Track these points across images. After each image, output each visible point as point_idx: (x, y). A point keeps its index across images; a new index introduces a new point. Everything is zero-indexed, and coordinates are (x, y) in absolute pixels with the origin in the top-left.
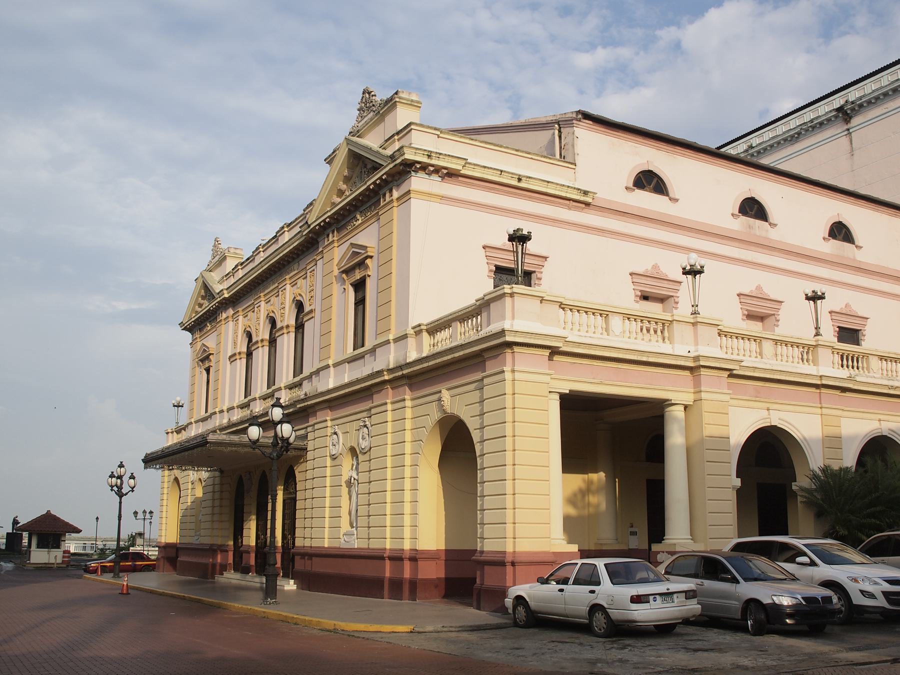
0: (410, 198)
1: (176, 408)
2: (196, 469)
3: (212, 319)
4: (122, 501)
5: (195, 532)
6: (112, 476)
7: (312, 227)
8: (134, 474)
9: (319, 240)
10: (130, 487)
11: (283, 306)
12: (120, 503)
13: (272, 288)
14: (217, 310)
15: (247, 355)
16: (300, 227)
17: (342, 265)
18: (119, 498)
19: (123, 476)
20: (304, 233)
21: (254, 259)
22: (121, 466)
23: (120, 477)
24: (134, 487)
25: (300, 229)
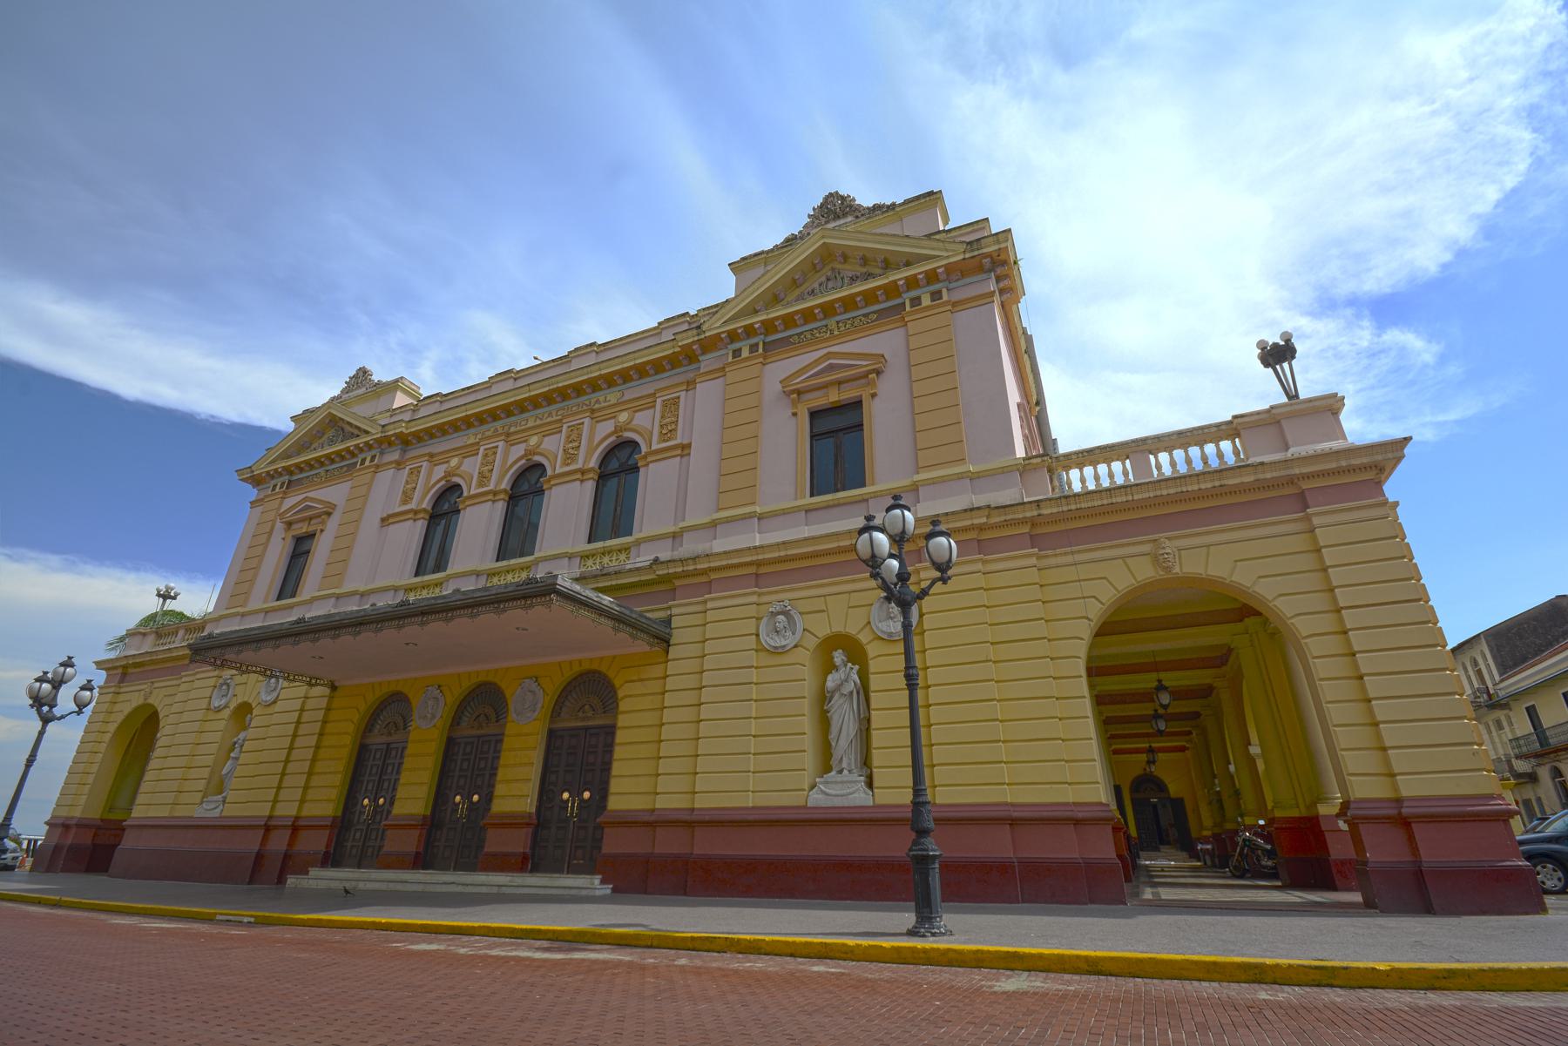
1: (161, 600)
3: (333, 466)
7: (707, 334)
8: (93, 683)
11: (576, 444)
12: (41, 733)
13: (531, 424)
14: (361, 450)
15: (431, 517)
16: (674, 334)
18: (41, 723)
19: (65, 683)
20: (680, 344)
21: (491, 386)
22: (68, 663)
23: (57, 684)
25: (673, 337)
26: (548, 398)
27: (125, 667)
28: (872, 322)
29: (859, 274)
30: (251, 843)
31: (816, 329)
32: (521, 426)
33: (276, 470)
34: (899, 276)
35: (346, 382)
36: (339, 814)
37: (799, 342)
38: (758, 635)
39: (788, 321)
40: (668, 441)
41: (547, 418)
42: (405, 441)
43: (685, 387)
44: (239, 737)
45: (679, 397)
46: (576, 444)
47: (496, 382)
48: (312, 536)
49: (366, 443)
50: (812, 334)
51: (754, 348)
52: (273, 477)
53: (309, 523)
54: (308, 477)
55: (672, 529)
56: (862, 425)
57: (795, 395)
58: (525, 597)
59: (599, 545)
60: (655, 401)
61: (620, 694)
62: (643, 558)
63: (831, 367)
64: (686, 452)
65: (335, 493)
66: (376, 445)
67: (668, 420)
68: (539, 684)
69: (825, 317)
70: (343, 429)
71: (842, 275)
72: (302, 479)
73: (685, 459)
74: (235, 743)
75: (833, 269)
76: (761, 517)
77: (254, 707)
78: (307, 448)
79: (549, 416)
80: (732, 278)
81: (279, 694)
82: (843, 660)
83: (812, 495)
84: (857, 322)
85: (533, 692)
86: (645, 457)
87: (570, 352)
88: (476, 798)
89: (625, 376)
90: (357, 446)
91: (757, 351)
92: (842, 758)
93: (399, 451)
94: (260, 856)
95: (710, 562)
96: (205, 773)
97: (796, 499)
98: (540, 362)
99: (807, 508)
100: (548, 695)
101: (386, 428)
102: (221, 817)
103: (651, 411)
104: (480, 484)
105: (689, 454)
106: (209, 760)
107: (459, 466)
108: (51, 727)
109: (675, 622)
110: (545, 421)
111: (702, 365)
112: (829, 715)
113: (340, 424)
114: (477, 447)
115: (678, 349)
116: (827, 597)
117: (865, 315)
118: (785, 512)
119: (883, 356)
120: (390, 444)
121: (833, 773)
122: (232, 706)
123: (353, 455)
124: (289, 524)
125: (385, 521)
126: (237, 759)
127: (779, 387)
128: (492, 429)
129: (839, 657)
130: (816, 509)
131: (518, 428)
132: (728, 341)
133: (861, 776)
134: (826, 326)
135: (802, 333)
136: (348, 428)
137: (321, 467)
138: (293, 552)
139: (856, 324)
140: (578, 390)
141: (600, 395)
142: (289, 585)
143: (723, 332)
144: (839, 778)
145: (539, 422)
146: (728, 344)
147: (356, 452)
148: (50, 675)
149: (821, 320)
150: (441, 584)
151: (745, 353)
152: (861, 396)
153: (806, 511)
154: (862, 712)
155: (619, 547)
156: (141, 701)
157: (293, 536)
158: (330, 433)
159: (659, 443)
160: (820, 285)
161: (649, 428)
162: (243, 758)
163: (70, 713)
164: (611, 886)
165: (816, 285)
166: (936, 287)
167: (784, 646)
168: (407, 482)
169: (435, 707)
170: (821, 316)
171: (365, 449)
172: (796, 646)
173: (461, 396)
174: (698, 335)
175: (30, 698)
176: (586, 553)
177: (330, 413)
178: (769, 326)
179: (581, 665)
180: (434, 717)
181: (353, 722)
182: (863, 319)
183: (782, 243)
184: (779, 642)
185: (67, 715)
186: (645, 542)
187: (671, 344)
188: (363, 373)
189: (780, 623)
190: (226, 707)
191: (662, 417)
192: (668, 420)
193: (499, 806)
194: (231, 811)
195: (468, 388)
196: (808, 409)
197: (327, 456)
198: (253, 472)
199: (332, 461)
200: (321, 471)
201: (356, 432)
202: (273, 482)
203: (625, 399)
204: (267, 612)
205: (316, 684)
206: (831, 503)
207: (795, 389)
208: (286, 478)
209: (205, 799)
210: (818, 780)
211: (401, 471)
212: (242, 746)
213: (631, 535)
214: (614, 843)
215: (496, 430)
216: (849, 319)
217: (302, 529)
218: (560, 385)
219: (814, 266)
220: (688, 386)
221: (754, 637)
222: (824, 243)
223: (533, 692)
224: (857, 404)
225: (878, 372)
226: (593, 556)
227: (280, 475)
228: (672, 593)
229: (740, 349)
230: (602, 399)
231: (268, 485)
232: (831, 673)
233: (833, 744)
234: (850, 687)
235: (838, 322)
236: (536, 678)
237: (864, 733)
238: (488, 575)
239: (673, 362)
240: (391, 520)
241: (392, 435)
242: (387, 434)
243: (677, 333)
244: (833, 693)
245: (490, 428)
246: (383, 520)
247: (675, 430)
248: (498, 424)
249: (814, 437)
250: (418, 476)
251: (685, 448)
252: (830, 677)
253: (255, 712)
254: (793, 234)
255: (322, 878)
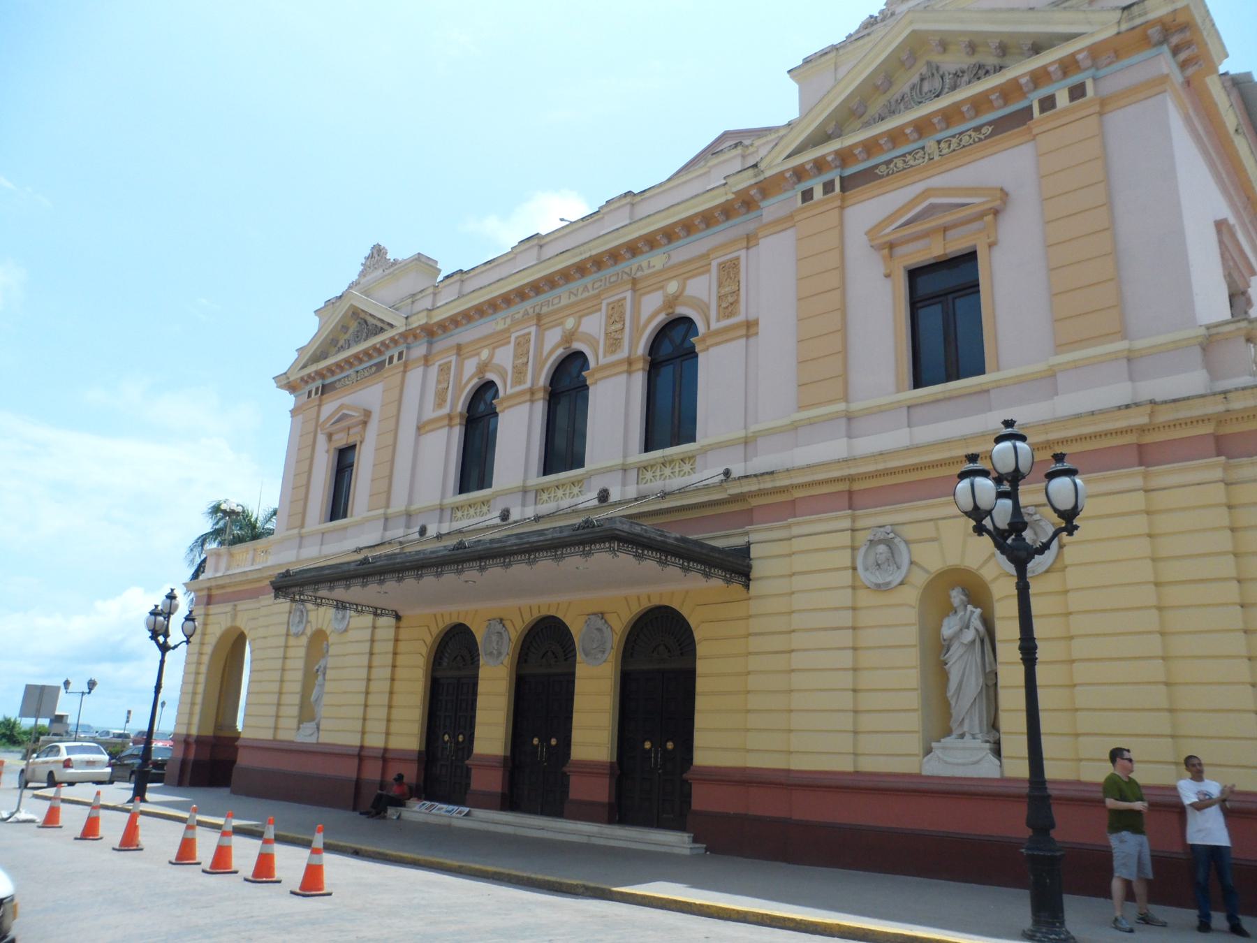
0: (1165, 91)
2: (359, 608)
3: (364, 366)
4: (167, 658)
5: (300, 722)
6: (154, 613)
7: (768, 174)
9: (762, 204)
10: (185, 635)
11: (618, 326)
12: (162, 662)
13: (564, 302)
14: (387, 347)
16: (725, 178)
17: (883, 233)
20: (734, 190)
22: (171, 597)
24: (191, 636)
25: (724, 182)
26: (581, 269)
27: (209, 589)
28: (986, 138)
29: (965, 67)
30: (348, 771)
31: (910, 153)
32: (553, 305)
33: (309, 376)
34: (1020, 69)
35: (362, 264)
36: (423, 748)
37: (888, 174)
38: (854, 569)
39: (870, 147)
40: (728, 316)
41: (582, 294)
42: (430, 332)
43: (745, 244)
44: (320, 664)
45: (738, 258)
46: (618, 326)
47: (521, 252)
48: (352, 447)
49: (392, 339)
50: (904, 161)
51: (828, 187)
52: (307, 382)
53: (348, 435)
54: (339, 380)
55: (742, 434)
56: (978, 285)
57: (886, 251)
58: (582, 543)
59: (656, 454)
60: (710, 264)
61: (697, 636)
62: (708, 472)
63: (932, 210)
64: (752, 331)
65: (371, 395)
66: (401, 341)
67: (727, 290)
68: (606, 622)
69: (921, 136)
70: (366, 322)
71: (941, 73)
72: (335, 382)
73: (752, 340)
74: (318, 670)
75: (929, 63)
76: (850, 417)
77: (328, 634)
78: (335, 346)
79: (584, 291)
80: (793, 88)
81: (349, 622)
82: (962, 600)
83: (917, 384)
84: (965, 139)
85: (599, 630)
86: (703, 340)
87: (601, 208)
88: (553, 742)
89: (669, 234)
90: (383, 343)
91: (833, 190)
92: (963, 719)
93: (426, 344)
94: (358, 784)
95: (791, 478)
96: (296, 699)
97: (898, 391)
98: (568, 223)
99: (909, 403)
100: (616, 634)
101: (410, 320)
102: (318, 744)
103: (707, 276)
104: (518, 379)
105: (757, 334)
106: (297, 687)
107: (492, 356)
108: (169, 654)
109: (755, 552)
110: (580, 297)
111: (765, 212)
112: (946, 667)
113: (362, 315)
114: (507, 335)
115: (733, 196)
116: (940, 522)
117: (978, 129)
118: (880, 410)
119: (1002, 190)
120: (415, 337)
121: (954, 736)
122: (309, 632)
123: (380, 352)
124: (330, 436)
125: (422, 428)
126: (322, 686)
127: (865, 238)
128: (522, 312)
129: (957, 597)
130: (922, 404)
131: (551, 308)
132: (795, 179)
133: (987, 742)
134: (923, 148)
135: (888, 163)
136: (370, 320)
137: (351, 367)
138: (338, 465)
139: (963, 143)
140: (614, 256)
141: (642, 260)
142: (338, 507)
143: (787, 170)
144: (960, 743)
145: (573, 299)
146: (796, 184)
147: (383, 349)
148: (160, 608)
149: (915, 141)
150: (488, 501)
151: (818, 193)
152: (975, 246)
153: (909, 407)
154: (987, 666)
155: (681, 456)
156: (229, 624)
157: (335, 448)
158: (354, 326)
159: (718, 320)
160: (913, 88)
161: (706, 299)
162: (329, 687)
163: (181, 643)
164: (705, 846)
165: (906, 89)
166: (1074, 80)
167: (889, 583)
168: (438, 382)
169: (500, 643)
170: (915, 135)
171: (392, 345)
172: (902, 583)
173: (482, 272)
174: (756, 176)
175: (149, 630)
176: (645, 464)
177: (351, 305)
178: (844, 157)
179: (649, 600)
180: (500, 654)
181: (422, 655)
182: (973, 134)
183: (857, 32)
184: (879, 578)
185: (179, 645)
186: (712, 449)
187: (722, 190)
188: (378, 252)
189: (881, 554)
190: (303, 633)
191: (720, 285)
192: (727, 290)
193: (580, 751)
194: (325, 738)
195: (489, 262)
196: (905, 268)
197: (356, 356)
198: (288, 378)
199: (361, 361)
200: (351, 372)
201: (380, 324)
202: (307, 388)
203: (672, 262)
204: (323, 534)
205: (381, 615)
206: (941, 396)
207: (885, 243)
208: (319, 383)
209: (301, 726)
210: (934, 744)
211: (431, 368)
212: (324, 674)
213: (692, 439)
214: (702, 799)
215: (526, 313)
216: (953, 136)
217: (341, 441)
218: (594, 252)
219: (902, 63)
220: (748, 242)
221: (851, 571)
222: (914, 32)
223: (599, 630)
224: (970, 257)
225: (996, 212)
226: (652, 466)
227: (314, 379)
228: (748, 516)
229: (811, 190)
230: (644, 264)
231: (302, 391)
232: (948, 615)
233: (953, 702)
234: (969, 635)
235: (939, 142)
236: (602, 614)
237: (992, 689)
238: (537, 491)
239: (727, 211)
240: (427, 428)
241: (417, 328)
242: (411, 327)
243: (729, 176)
244: (951, 639)
245: (519, 309)
246: (419, 428)
247: (737, 302)
248: (527, 305)
249: (916, 303)
250: (449, 374)
251: (750, 327)
252: (946, 622)
253: (331, 640)
254: (871, 17)
255: (417, 811)
